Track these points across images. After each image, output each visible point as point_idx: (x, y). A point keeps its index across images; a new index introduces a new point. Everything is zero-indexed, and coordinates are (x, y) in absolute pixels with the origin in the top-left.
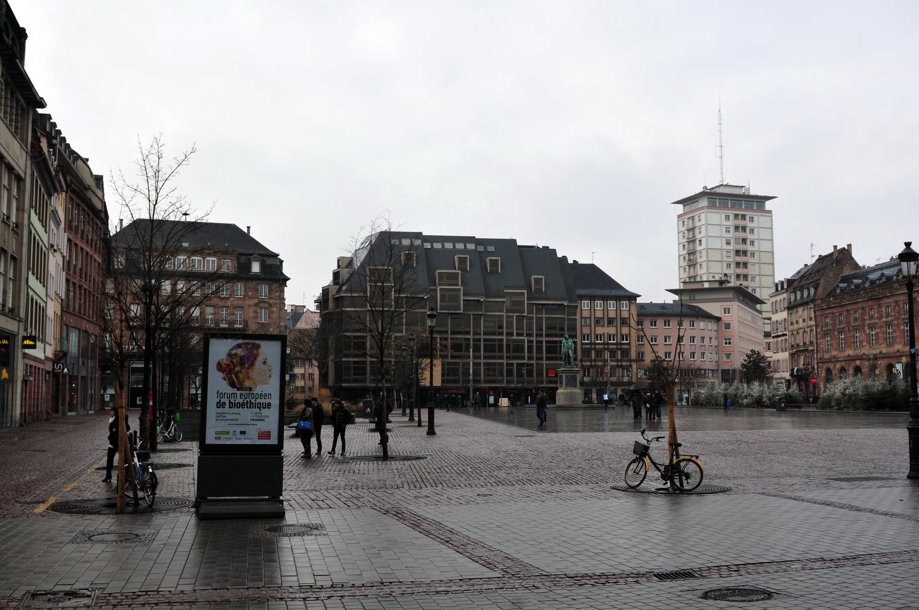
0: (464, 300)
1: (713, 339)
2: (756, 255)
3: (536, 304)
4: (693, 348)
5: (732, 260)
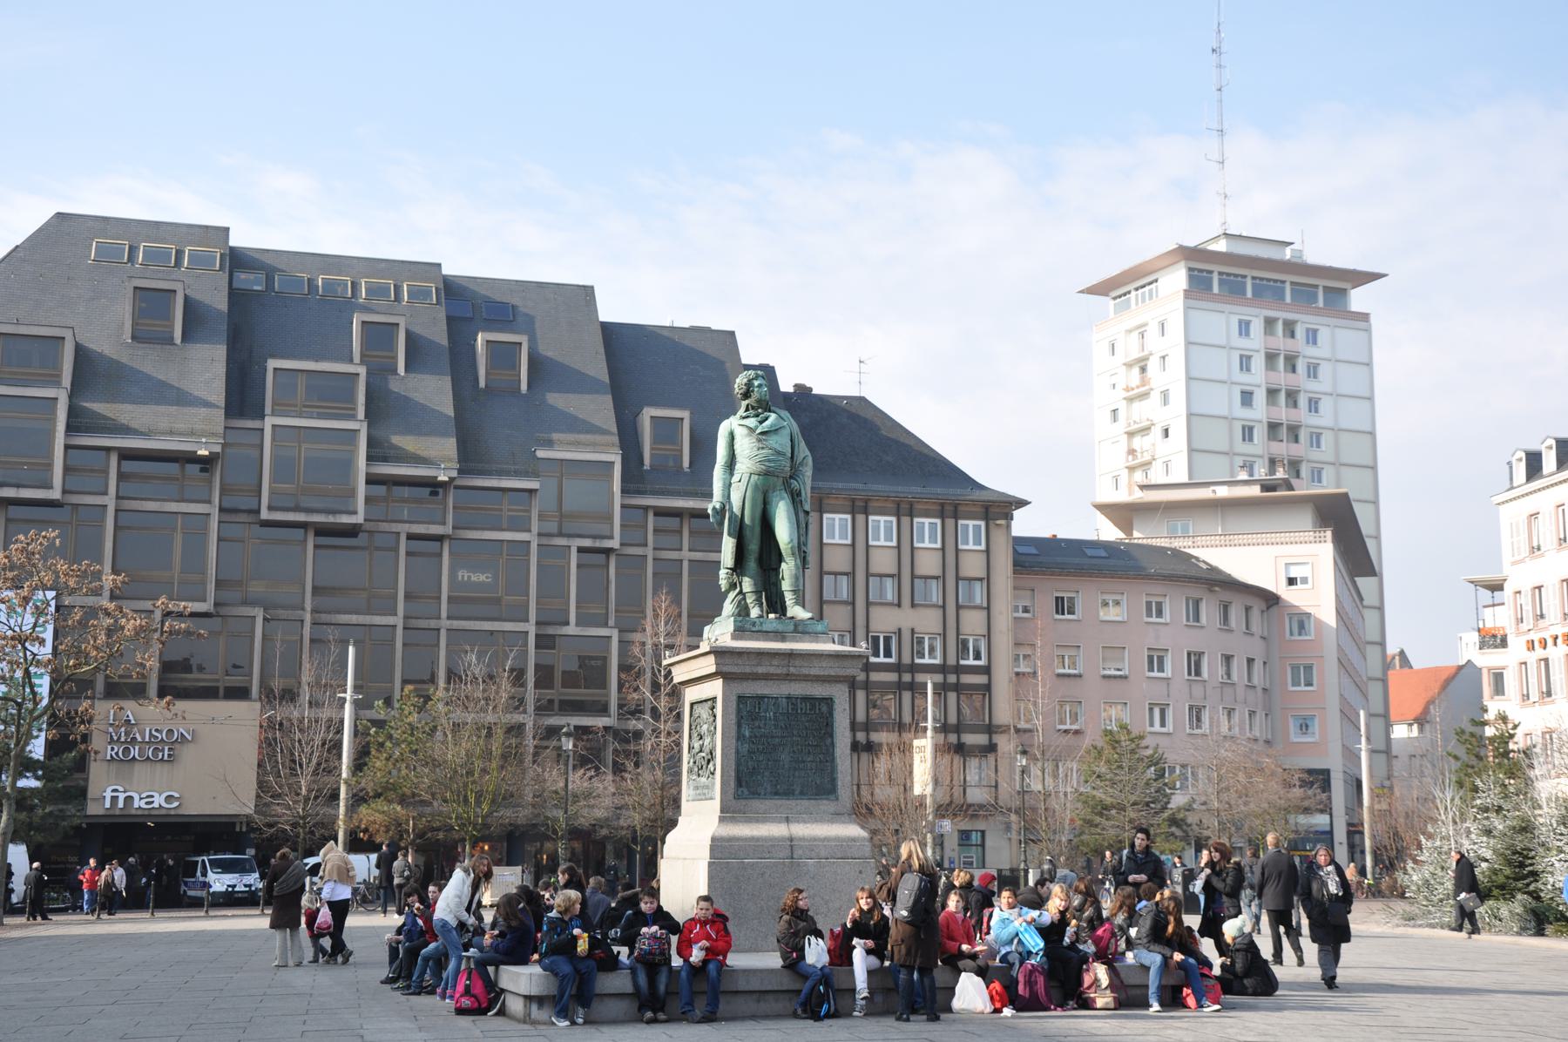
0: (372, 480)
1: (1258, 666)
2: (1327, 439)
3: (660, 513)
4: (1198, 691)
5: (1259, 451)
